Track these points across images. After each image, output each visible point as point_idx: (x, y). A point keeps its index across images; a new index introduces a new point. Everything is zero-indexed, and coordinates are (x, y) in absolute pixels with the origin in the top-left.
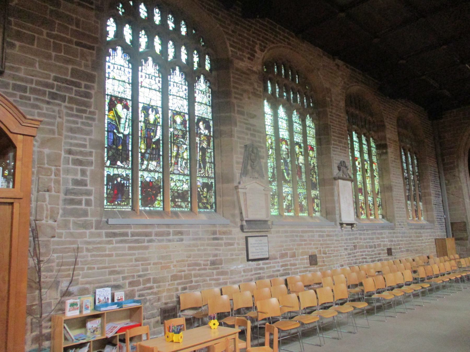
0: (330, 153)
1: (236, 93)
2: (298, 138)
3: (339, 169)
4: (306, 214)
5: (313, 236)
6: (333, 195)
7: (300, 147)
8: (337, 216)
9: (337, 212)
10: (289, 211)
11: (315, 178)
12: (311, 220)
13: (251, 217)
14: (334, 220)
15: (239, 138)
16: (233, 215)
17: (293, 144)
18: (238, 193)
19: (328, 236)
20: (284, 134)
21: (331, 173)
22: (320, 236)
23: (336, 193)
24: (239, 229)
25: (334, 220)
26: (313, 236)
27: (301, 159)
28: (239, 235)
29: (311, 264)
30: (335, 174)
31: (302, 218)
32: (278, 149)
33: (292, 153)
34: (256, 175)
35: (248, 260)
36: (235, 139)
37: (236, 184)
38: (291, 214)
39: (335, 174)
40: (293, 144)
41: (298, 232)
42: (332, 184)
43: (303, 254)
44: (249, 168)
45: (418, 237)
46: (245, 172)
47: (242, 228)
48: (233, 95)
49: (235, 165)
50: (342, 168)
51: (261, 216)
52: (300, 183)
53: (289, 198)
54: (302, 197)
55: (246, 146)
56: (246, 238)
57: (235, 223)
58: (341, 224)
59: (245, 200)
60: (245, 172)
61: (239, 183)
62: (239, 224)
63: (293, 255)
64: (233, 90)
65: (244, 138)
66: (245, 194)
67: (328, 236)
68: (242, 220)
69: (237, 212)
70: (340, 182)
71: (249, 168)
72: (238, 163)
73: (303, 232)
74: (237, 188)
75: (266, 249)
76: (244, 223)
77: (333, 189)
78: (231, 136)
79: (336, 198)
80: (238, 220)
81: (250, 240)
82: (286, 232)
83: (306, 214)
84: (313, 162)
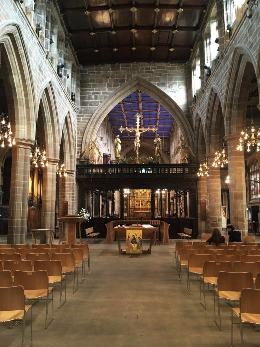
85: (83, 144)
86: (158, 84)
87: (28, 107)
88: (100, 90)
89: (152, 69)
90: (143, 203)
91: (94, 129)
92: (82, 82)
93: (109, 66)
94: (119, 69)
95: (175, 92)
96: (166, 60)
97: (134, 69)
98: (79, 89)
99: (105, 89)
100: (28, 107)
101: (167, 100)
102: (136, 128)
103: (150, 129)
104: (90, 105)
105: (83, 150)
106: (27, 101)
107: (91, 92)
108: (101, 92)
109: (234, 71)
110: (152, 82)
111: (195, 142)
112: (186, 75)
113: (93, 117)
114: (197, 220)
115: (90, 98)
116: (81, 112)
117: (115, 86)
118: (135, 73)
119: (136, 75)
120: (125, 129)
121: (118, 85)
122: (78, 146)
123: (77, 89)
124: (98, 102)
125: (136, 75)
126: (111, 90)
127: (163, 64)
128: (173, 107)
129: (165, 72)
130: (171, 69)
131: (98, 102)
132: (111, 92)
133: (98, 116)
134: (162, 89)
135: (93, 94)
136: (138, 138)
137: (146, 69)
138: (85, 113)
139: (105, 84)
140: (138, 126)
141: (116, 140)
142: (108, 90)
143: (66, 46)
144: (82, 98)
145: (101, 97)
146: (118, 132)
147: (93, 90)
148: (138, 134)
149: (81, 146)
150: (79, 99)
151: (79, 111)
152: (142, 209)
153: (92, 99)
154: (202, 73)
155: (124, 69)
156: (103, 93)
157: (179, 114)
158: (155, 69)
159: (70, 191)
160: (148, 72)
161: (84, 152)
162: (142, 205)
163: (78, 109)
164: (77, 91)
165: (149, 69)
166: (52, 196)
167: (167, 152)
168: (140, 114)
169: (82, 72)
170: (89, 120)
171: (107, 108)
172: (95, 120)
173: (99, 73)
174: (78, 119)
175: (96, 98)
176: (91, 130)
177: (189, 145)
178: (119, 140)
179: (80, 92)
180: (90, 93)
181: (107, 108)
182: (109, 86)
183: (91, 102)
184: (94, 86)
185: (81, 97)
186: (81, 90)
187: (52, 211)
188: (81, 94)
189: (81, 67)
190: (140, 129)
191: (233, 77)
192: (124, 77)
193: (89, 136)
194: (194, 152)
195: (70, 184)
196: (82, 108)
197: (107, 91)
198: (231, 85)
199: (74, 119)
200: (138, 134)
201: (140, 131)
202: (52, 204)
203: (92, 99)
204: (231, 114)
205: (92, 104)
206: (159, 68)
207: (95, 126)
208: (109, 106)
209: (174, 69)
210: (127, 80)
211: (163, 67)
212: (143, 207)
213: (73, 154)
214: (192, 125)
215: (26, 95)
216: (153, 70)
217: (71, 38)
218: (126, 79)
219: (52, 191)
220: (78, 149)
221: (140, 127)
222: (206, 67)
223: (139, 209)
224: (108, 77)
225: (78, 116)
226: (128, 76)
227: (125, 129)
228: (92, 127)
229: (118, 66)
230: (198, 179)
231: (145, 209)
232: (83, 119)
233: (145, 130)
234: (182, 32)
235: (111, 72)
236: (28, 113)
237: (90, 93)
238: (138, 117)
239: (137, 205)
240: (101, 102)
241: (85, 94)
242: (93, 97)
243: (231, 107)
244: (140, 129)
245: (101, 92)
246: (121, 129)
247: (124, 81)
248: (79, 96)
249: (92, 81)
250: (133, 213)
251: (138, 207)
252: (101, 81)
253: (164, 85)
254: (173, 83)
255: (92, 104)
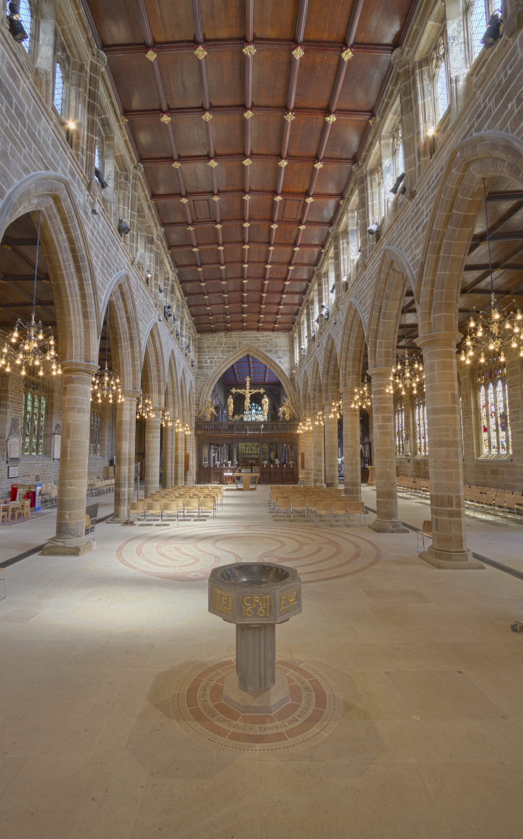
0: (52, 420)
1: (11, 391)
2: (36, 411)
3: (56, 428)
4: (35, 454)
5: (38, 466)
6: (51, 443)
7: (36, 416)
8: (52, 455)
9: (52, 453)
10: (27, 452)
11: (42, 433)
12: (38, 457)
13: (12, 456)
14: (50, 457)
15: (10, 415)
16: (3, 456)
17: (33, 414)
18: (7, 444)
19: (46, 465)
20: (29, 408)
21: (52, 431)
22: (42, 466)
23: (53, 442)
24: (5, 462)
25: (50, 457)
26: (38, 466)
27: (36, 423)
28: (4, 465)
29: (36, 480)
30: (53, 431)
31: (34, 456)
32: (25, 418)
33: (32, 419)
34: (16, 435)
35: (8, 478)
36: (8, 416)
37: (6, 440)
38: (27, 453)
39: (53, 431)
40: (33, 414)
41: (32, 464)
42: (51, 437)
43: (33, 475)
44: (13, 431)
45: (94, 465)
46: (11, 434)
47: (7, 462)
48: (10, 392)
49: (7, 430)
50: (58, 428)
51: (17, 455)
52: (34, 436)
53: (28, 445)
54: (34, 444)
55: (13, 419)
56: (9, 467)
57: (4, 459)
58: (54, 459)
59: (10, 448)
60: (11, 434)
61: (8, 439)
62: (6, 460)
63: (28, 476)
64: (9, 389)
65: (12, 415)
66: (10, 445)
67: (46, 465)
68: (7, 457)
69: (5, 454)
70: (56, 436)
71: (13, 431)
72: (8, 428)
73: (34, 463)
74: (7, 441)
75: (17, 472)
76: (9, 460)
77: (51, 440)
78: (6, 414)
79: (52, 445)
80: (5, 458)
81: (11, 468)
82: (26, 464)
83: (35, 454)
84: (42, 424)
85: (200, 403)
86: (265, 351)
87: (174, 396)
88: (215, 355)
89: (260, 337)
90: (253, 448)
91: (209, 389)
92: (199, 348)
93: (222, 334)
94: (231, 337)
95: (280, 358)
96: (273, 330)
97: (244, 337)
98: (197, 355)
99: (219, 355)
100: (174, 396)
101: (273, 364)
102: (246, 389)
103: (259, 391)
104: (206, 369)
105: (200, 409)
106: (173, 392)
107: (207, 357)
108: (216, 357)
109: (315, 368)
110: (260, 349)
111: (297, 402)
112: (290, 343)
113: (208, 379)
114: (297, 468)
115: (206, 362)
116: (198, 375)
117: (228, 352)
118: (245, 340)
119: (245, 342)
120: (236, 391)
121: (231, 351)
122: (196, 405)
123: (195, 355)
124: (213, 366)
125: (245, 342)
126: (224, 355)
127: (270, 333)
128: (279, 371)
129: (272, 340)
130: (277, 337)
131: (213, 366)
132: (225, 357)
133: (212, 378)
134: (269, 355)
135: (208, 358)
136: (249, 399)
137: (255, 337)
138: (202, 376)
139: (219, 350)
140: (248, 387)
141: (229, 399)
142: (222, 355)
143: (190, 328)
144: (200, 362)
145: (216, 362)
146: (232, 394)
147: (208, 355)
148: (248, 395)
149: (198, 405)
150: (197, 364)
151: (196, 374)
152: (251, 454)
153: (207, 363)
154: (300, 352)
155: (235, 337)
156: (218, 358)
157: (283, 376)
158: (263, 337)
159: (190, 444)
160: (257, 340)
161: (201, 410)
162: (252, 450)
163: (196, 372)
164: (195, 358)
165: (258, 337)
166: (182, 452)
167: (277, 396)
168: (250, 377)
169: (198, 339)
170: (205, 381)
171: (220, 371)
172: (210, 382)
173: (214, 340)
174: (196, 381)
175: (211, 362)
176: (207, 391)
177: (292, 404)
178: (232, 400)
179: (197, 357)
180: (206, 358)
181: (220, 371)
182: (223, 351)
183: (207, 366)
184: (209, 352)
185: (198, 361)
186: (199, 356)
187: (182, 463)
188: (198, 359)
189: (198, 336)
190: (250, 391)
191: (315, 371)
192: (235, 344)
193: (205, 395)
194: (296, 411)
195: (190, 439)
196: (199, 371)
197: (221, 356)
198: (314, 376)
199: (194, 383)
200: (248, 395)
201: (250, 392)
202: (182, 458)
203: (207, 363)
204: (315, 395)
205: (208, 367)
206: (266, 336)
207: (210, 387)
208: (222, 369)
209: (279, 337)
210: (238, 347)
211: (270, 336)
212: (253, 452)
213: (192, 413)
214: (294, 387)
215: (173, 388)
216: (261, 338)
217: (194, 322)
218: (237, 345)
219: (182, 448)
220: (196, 408)
221: (250, 389)
222: (302, 349)
223: (248, 454)
224: (222, 344)
225: (196, 378)
226: (239, 343)
227: (236, 391)
228: (208, 387)
229: (231, 335)
230: (298, 435)
231: (255, 454)
232: (201, 381)
233: (254, 391)
234: (284, 317)
235: (224, 340)
236: (174, 399)
237: (205, 358)
238: (248, 379)
239: (246, 450)
240: (215, 366)
241: (202, 358)
242: (209, 361)
243: (315, 390)
244: (250, 391)
245: (216, 357)
246: (234, 391)
247: (235, 347)
248: (197, 360)
249: (208, 347)
250: (242, 459)
251: (247, 452)
252: (216, 348)
253: (270, 351)
254: (279, 350)
255: (208, 367)
